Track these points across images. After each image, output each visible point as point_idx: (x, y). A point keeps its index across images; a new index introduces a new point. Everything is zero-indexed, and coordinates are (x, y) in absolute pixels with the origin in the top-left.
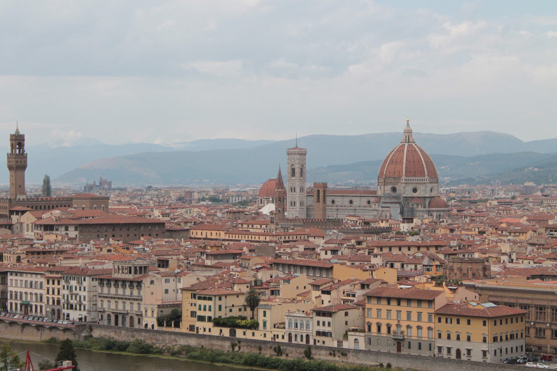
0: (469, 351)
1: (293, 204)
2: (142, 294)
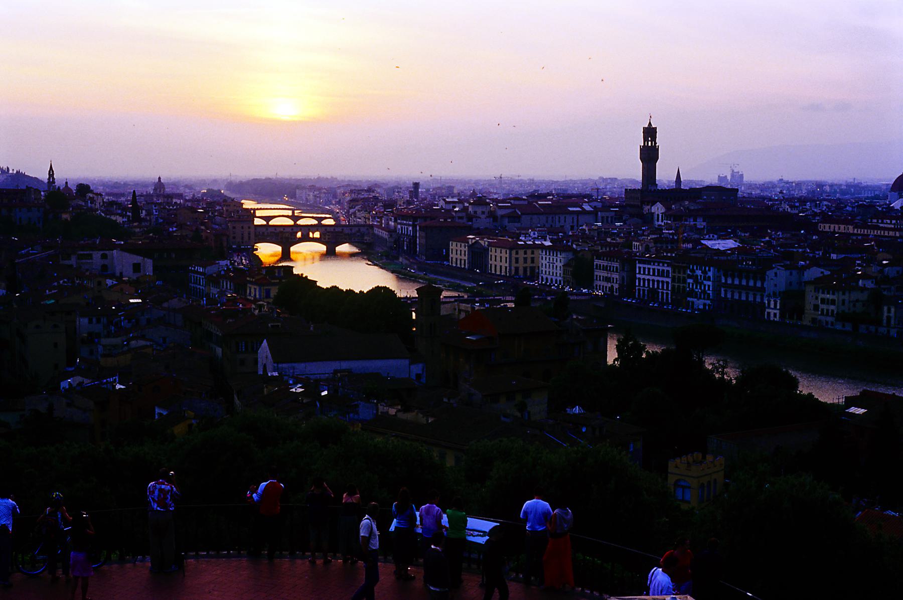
2: (765, 286)
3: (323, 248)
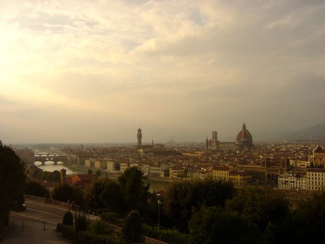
0: (237, 183)
1: (214, 146)
3: (53, 163)
